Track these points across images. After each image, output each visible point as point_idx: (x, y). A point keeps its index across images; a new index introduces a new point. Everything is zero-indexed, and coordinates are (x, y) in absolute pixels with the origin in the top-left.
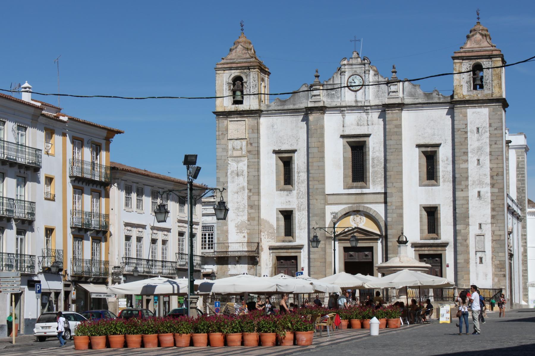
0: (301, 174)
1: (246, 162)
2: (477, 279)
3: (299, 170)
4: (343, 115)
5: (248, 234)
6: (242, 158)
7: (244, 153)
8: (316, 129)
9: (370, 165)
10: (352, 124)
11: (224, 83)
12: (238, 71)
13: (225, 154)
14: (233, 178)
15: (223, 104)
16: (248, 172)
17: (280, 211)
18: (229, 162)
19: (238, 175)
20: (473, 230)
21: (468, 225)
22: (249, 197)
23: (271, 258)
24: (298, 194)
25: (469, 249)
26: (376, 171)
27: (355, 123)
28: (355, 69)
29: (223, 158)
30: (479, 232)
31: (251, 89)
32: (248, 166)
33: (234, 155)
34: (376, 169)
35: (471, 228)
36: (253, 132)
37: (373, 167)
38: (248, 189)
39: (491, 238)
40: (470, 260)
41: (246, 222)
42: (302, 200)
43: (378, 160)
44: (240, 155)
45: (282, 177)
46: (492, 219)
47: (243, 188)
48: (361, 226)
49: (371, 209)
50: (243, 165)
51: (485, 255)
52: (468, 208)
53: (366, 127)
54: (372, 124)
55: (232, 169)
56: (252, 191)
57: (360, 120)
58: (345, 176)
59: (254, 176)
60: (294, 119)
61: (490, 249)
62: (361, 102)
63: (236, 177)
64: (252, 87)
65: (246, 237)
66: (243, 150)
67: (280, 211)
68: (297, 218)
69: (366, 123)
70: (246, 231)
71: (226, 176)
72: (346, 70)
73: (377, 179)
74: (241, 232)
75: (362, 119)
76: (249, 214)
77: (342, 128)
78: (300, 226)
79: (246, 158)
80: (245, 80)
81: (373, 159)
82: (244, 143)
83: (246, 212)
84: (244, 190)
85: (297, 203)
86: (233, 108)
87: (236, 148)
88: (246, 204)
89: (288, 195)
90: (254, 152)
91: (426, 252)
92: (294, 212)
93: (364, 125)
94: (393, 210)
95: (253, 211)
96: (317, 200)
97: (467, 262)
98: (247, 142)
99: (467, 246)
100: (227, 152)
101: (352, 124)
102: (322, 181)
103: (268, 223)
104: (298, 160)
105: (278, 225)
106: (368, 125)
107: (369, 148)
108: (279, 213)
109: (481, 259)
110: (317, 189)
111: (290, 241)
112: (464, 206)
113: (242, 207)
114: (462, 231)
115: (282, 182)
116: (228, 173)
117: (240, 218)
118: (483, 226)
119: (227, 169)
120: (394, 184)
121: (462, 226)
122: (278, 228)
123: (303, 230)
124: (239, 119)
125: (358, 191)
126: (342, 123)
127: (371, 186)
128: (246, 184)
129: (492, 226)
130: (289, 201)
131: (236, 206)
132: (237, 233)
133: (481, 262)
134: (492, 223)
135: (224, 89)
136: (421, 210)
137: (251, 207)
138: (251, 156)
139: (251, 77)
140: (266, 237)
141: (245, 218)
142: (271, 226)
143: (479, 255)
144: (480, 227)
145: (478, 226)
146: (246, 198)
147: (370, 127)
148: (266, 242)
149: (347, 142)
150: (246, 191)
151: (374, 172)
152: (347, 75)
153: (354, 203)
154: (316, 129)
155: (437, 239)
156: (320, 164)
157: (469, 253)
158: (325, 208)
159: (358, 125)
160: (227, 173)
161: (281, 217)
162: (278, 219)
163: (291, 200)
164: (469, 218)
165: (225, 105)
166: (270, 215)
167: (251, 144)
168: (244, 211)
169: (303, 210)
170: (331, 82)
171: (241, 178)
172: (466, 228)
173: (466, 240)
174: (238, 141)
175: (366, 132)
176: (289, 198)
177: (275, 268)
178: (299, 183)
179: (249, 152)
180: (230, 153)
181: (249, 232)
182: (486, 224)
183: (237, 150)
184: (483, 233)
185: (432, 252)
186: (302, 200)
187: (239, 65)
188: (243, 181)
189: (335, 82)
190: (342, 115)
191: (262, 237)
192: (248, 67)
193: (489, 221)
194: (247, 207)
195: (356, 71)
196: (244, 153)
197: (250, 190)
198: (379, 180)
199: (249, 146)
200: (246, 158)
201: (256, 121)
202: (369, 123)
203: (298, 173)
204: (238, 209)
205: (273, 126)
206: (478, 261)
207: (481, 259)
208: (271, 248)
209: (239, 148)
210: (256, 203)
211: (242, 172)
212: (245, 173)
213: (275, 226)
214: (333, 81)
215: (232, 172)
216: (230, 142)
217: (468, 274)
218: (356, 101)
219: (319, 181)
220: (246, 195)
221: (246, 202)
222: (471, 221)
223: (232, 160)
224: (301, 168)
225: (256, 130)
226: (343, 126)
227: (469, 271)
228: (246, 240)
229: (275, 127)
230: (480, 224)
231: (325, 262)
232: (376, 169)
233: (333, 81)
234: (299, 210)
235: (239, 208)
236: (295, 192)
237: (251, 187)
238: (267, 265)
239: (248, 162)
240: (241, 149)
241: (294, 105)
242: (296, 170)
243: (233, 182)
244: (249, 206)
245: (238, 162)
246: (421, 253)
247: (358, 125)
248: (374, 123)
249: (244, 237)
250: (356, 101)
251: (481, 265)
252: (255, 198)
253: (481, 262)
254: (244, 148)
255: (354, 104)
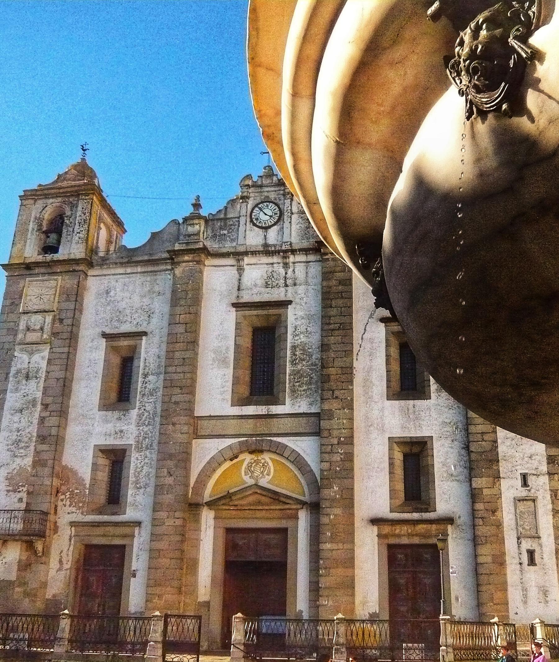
0: (151, 378)
1: (46, 353)
2: (525, 603)
3: (146, 371)
4: (240, 270)
5: (29, 493)
6: (41, 347)
7: (45, 336)
8: (186, 291)
9: (288, 359)
10: (256, 285)
11: (32, 219)
12: (60, 199)
13: (10, 338)
14: (18, 382)
15: (23, 253)
16: (48, 372)
17: (101, 451)
18: (16, 354)
19: (27, 377)
20: (510, 489)
21: (497, 477)
22: (42, 420)
23: (72, 548)
24: (140, 416)
25: (502, 532)
26: (298, 372)
27: (260, 282)
28: (266, 194)
29: (6, 346)
30: (522, 493)
31: (77, 226)
32: (49, 361)
33: (28, 340)
34: (299, 367)
35: (504, 484)
36: (68, 300)
37: (293, 363)
38: (42, 404)
39: (550, 507)
40: (508, 558)
41: (29, 469)
42: (146, 429)
43: (304, 350)
44: (39, 340)
45: (115, 385)
46: (548, 463)
47: (34, 402)
48: (263, 482)
49: (287, 446)
50: (40, 360)
51: (541, 545)
52: (496, 441)
53: (282, 289)
54: (295, 284)
55: (19, 366)
56: (50, 408)
57: (271, 276)
58: (236, 381)
59: (58, 379)
60: (149, 279)
61: (551, 531)
62: (275, 246)
63: (24, 382)
64: (77, 224)
65: (25, 500)
66: (45, 330)
67: (101, 451)
68: (132, 465)
69: (282, 281)
70: (25, 489)
71: (7, 378)
72: (251, 195)
73: (299, 386)
74: (15, 491)
75: (275, 274)
76: (37, 453)
77: (235, 293)
78: (137, 482)
79: (48, 347)
80: (68, 213)
81: (294, 347)
82: (49, 318)
83: (32, 448)
84: (34, 406)
85: (136, 433)
86: (40, 258)
87: (33, 327)
88: (35, 434)
89: (119, 419)
90: (65, 336)
91: (405, 541)
92: (128, 453)
93: (278, 286)
94: (332, 445)
95: (45, 447)
96: (174, 424)
97: (500, 561)
98: (55, 316)
99: (499, 525)
100: (16, 335)
101: (256, 285)
102: (190, 388)
103: (75, 473)
104: (147, 352)
105: (93, 479)
106: (286, 286)
107: (286, 327)
108: (100, 454)
109: (531, 553)
110: (176, 403)
111: (113, 514)
112: (486, 437)
113: (26, 439)
114: (486, 492)
115: (113, 396)
116: (11, 374)
117: (18, 461)
118: (531, 480)
119: (10, 367)
120: (337, 393)
121: (484, 479)
122: (92, 485)
123: (142, 491)
124: (46, 277)
125: (261, 410)
126: (236, 283)
127: (288, 400)
128: (39, 395)
129: (550, 480)
130: (121, 431)
131: (14, 437)
132: (8, 491)
133: (532, 562)
134: (550, 474)
135: (30, 229)
136: (391, 449)
137: (42, 438)
138: (57, 342)
139: (80, 208)
140: (68, 503)
141: (29, 461)
142: (80, 482)
143: (526, 545)
144: (525, 483)
145: (519, 482)
146: (36, 422)
147: (290, 289)
148: (67, 515)
149: (245, 317)
150: (39, 407)
151: (294, 373)
152: (251, 203)
153: (251, 436)
154: (186, 291)
155: (427, 511)
156: (188, 355)
157: (502, 541)
158: (190, 443)
159: (267, 285)
160: (8, 374)
161: (103, 461)
162: (95, 466)
163: (124, 428)
164: (498, 461)
165: (26, 255)
166: (81, 458)
167: (61, 321)
168: (28, 447)
169: (147, 448)
170: (222, 216)
171: (32, 383)
172: (494, 483)
173: (494, 512)
174: (39, 317)
175: (282, 298)
176: (120, 426)
177: (78, 570)
178: (144, 395)
179: (55, 334)
180: (20, 336)
181: (31, 490)
182: (538, 476)
183: (34, 330)
184: (532, 494)
185: (416, 540)
186: (146, 429)
187: (61, 191)
188: (35, 389)
189: (228, 216)
190: (238, 270)
191: (60, 504)
192: (76, 191)
193: (544, 468)
194: (34, 439)
195: (268, 197)
196: (45, 336)
197: (46, 406)
198: (305, 388)
199: (57, 325)
200: (48, 347)
201: (76, 282)
202: (289, 282)
203: (146, 376)
204: (17, 442)
205: (107, 292)
206: (525, 558)
207: (531, 553)
208: (72, 524)
209: (38, 327)
210: (54, 431)
211: (37, 372)
212: (42, 375)
213: (88, 482)
214: (225, 214)
215: (18, 372)
216: (24, 318)
217: (506, 590)
218: (266, 245)
219: (181, 388)
220: (37, 415)
221: (34, 430)
222: (503, 467)
223: (22, 350)
224: (152, 366)
225: (75, 296)
226: (239, 290)
227: (506, 583)
228: (23, 506)
229: (112, 294)
230: (524, 477)
231: (182, 559)
232: (299, 367)
233: (225, 214)
234: (139, 449)
235: (19, 440)
236: (134, 413)
237: (49, 400)
238: (61, 562)
239: (51, 352)
240: (42, 329)
241: (151, 254)
242: (141, 372)
243: (17, 390)
244: (38, 436)
245: (31, 353)
246: (392, 541)
247: (267, 285)
248: (298, 282)
249: (20, 500)
250: (266, 245)
251: (531, 567)
252: (53, 421)
253: (532, 562)
254: (47, 328)
255: (261, 249)
